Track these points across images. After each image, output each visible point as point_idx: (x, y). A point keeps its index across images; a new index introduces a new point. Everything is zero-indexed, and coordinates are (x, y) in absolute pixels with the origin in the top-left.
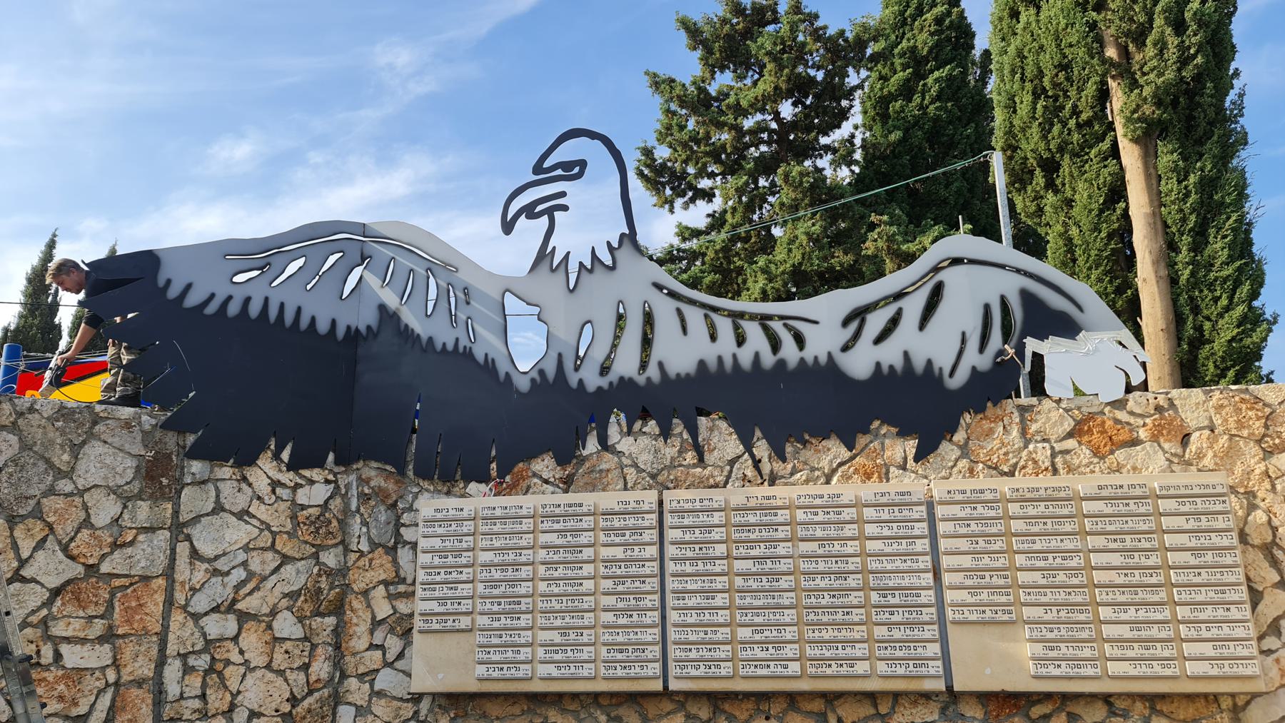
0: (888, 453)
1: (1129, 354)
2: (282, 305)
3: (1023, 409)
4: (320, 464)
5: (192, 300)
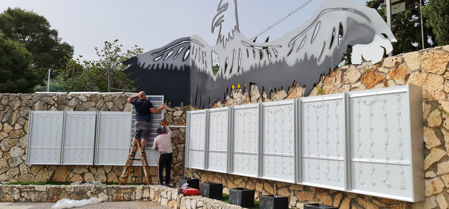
0: (298, 93)
1: (387, 41)
2: (167, 65)
3: (344, 71)
4: (179, 106)
5: (145, 67)
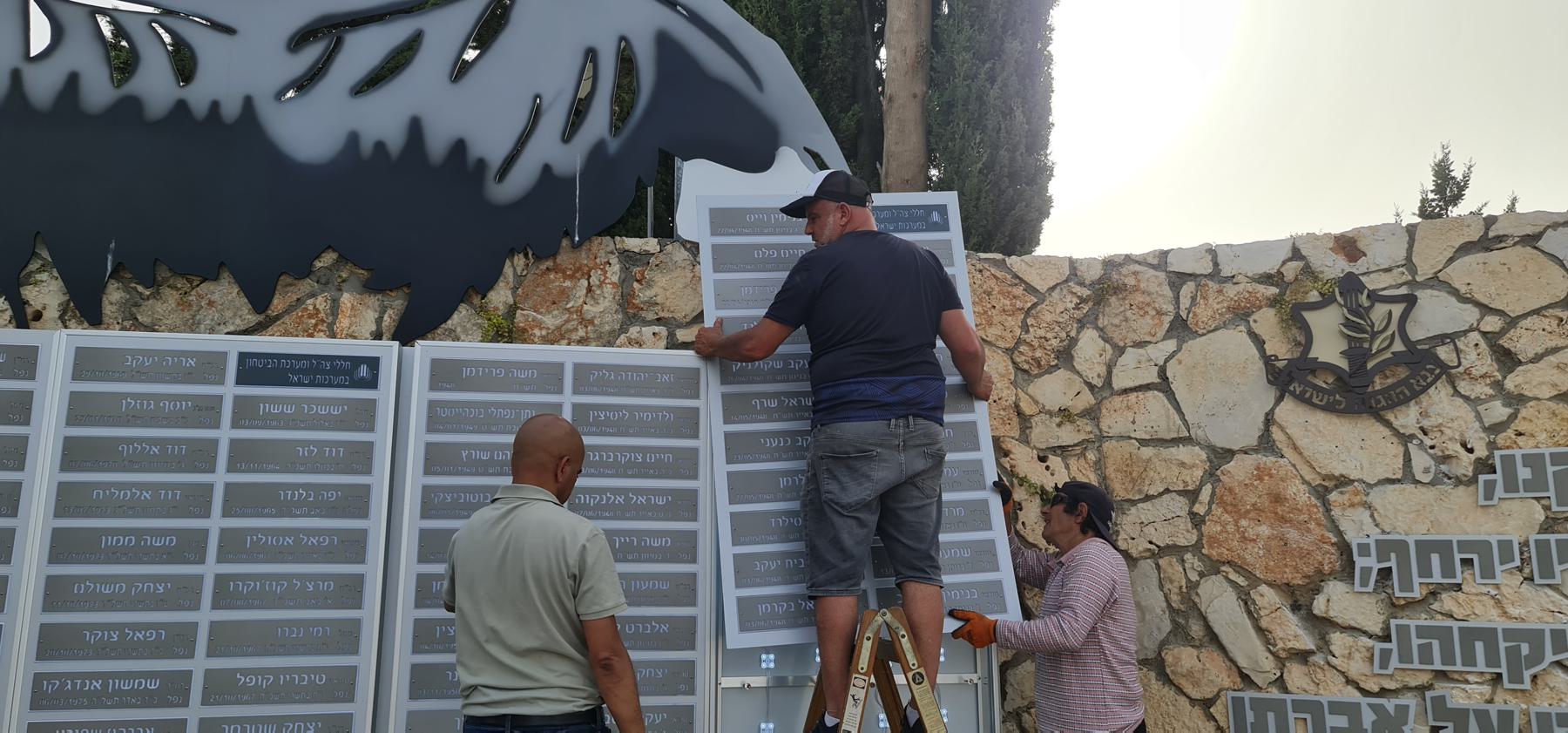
0: (343, 322)
3: (627, 257)
